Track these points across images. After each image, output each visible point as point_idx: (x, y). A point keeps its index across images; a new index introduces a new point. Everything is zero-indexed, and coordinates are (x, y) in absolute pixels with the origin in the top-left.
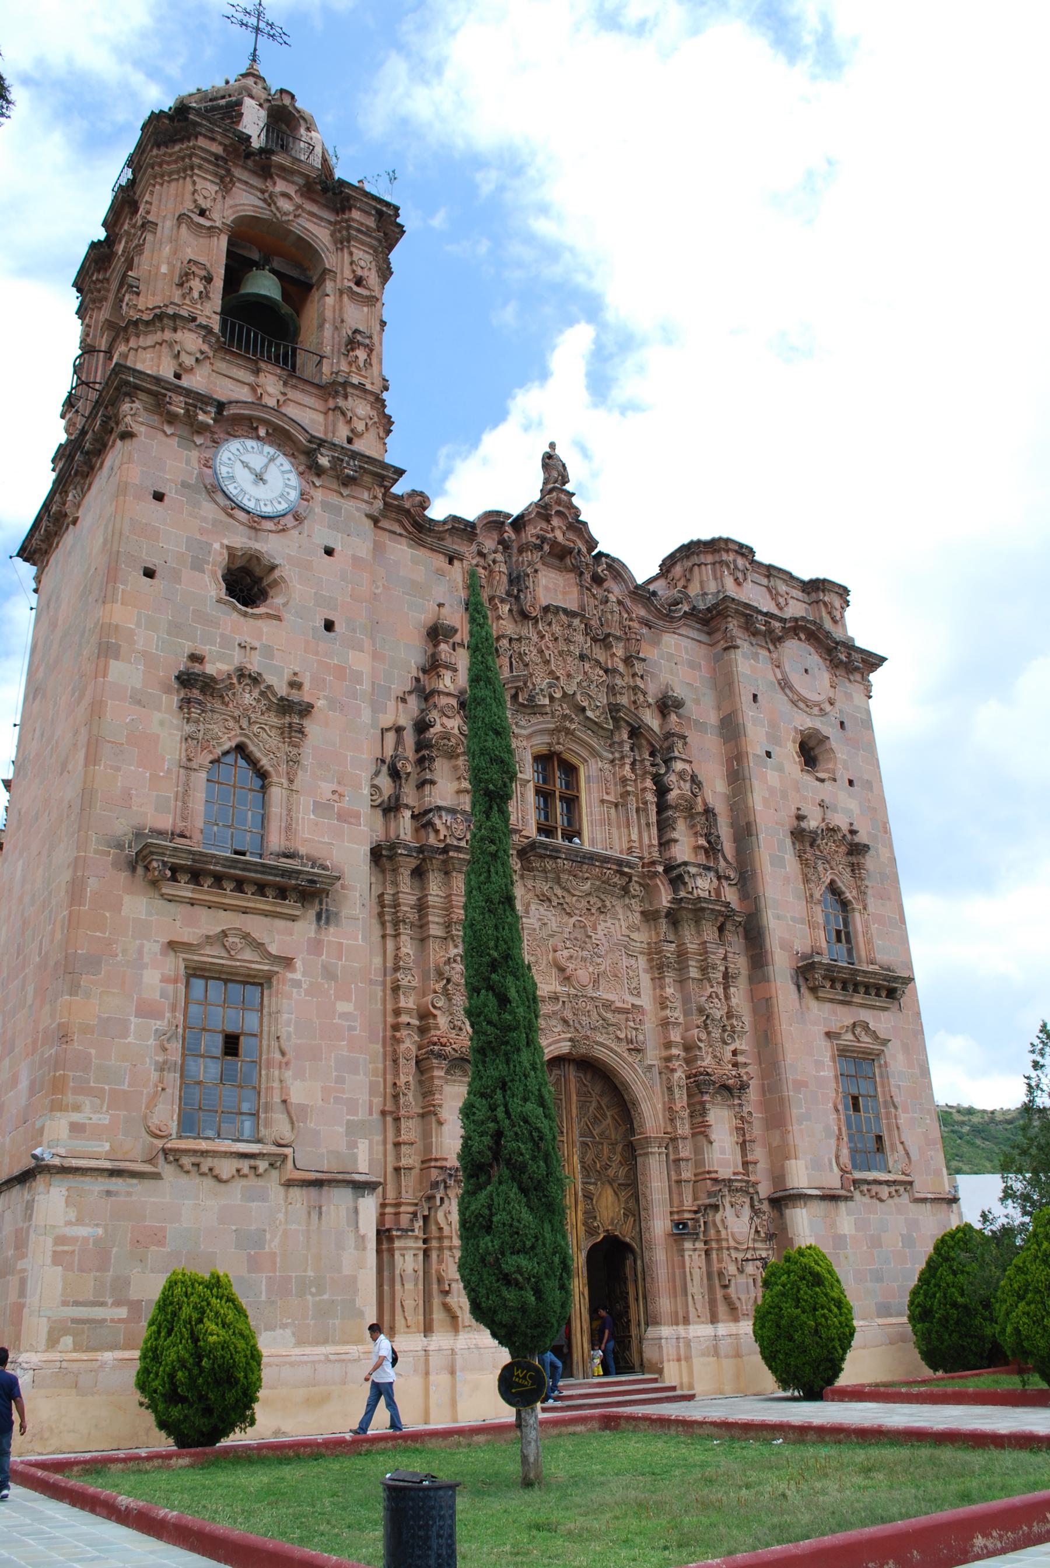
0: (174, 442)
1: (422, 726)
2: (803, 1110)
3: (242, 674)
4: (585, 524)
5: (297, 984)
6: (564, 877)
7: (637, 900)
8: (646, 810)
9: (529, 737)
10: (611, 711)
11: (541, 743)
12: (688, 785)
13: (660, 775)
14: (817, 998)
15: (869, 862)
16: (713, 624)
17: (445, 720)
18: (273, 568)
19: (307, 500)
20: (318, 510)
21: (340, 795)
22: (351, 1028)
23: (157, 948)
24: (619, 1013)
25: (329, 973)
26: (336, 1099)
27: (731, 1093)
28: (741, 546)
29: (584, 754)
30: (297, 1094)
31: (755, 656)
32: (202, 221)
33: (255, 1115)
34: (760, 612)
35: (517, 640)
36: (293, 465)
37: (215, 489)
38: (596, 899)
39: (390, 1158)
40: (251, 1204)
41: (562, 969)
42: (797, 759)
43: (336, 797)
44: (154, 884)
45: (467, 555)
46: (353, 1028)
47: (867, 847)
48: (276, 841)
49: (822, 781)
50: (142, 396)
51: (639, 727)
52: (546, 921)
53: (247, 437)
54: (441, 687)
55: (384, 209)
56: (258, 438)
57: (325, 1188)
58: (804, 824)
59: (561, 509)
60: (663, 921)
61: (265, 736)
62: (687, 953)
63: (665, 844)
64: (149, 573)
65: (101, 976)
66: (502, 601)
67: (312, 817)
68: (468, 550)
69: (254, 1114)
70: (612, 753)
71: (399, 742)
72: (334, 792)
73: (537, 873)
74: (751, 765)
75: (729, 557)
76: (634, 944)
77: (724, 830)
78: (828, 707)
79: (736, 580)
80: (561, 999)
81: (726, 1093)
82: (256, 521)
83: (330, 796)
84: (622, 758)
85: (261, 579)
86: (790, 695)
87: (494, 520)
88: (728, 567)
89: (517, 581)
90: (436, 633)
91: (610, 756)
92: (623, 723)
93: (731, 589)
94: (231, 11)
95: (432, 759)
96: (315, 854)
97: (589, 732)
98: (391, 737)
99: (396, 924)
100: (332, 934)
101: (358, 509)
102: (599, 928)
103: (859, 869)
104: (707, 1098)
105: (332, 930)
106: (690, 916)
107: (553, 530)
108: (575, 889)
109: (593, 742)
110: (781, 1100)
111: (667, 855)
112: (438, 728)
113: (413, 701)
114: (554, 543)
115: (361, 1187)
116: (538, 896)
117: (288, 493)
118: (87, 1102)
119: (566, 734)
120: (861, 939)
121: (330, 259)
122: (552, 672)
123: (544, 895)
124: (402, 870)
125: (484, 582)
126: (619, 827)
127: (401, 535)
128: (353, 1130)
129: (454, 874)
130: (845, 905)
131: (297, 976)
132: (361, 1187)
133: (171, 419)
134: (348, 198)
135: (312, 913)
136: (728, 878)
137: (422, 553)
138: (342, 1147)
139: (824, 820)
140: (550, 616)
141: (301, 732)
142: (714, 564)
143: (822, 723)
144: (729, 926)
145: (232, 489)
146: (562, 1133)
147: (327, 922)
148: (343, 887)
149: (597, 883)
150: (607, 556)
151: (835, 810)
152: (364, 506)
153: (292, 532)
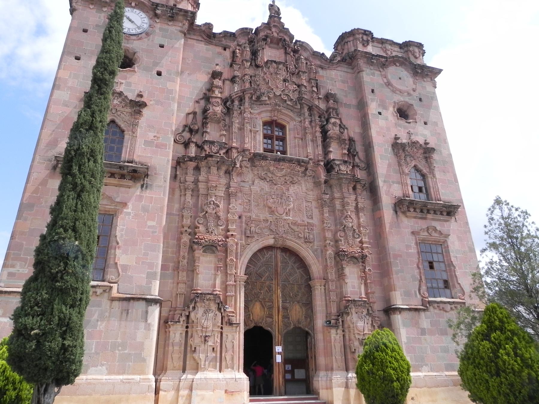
0: (94, 11)
1: (205, 111)
2: (399, 268)
4: (287, 29)
5: (129, 214)
6: (272, 168)
7: (311, 177)
8: (316, 140)
9: (259, 114)
10: (298, 100)
11: (266, 116)
12: (338, 128)
13: (324, 125)
14: (407, 217)
15: (435, 156)
16: (353, 64)
17: (214, 107)
18: (135, 53)
19: (152, 28)
20: (157, 31)
21: (158, 138)
22: (153, 232)
24: (301, 226)
25: (145, 209)
26: (143, 263)
27: (358, 260)
28: (365, 31)
29: (288, 119)
31: (373, 74)
35: (254, 76)
36: (147, 16)
38: (289, 178)
39: (175, 290)
40: (93, 308)
41: (270, 208)
42: (395, 115)
43: (156, 138)
45: (232, 46)
47: (433, 149)
49: (410, 123)
51: (312, 106)
52: (263, 188)
54: (214, 95)
56: (132, 7)
58: (399, 141)
59: (276, 24)
60: (323, 186)
61: (123, 116)
62: (335, 198)
63: (326, 153)
65: (33, 212)
66: (247, 61)
67: (143, 146)
68: (233, 45)
69: (102, 269)
70: (300, 118)
72: (154, 136)
73: (259, 168)
74: (370, 118)
75: (361, 36)
76: (310, 196)
77: (359, 148)
78: (412, 92)
79: (363, 45)
80: (269, 220)
81: (355, 260)
83: (153, 138)
84: (304, 119)
85: (132, 59)
86: (392, 88)
87: (245, 31)
88: (359, 40)
89: (254, 53)
91: (300, 119)
92: (305, 105)
93: (360, 48)
95: (207, 123)
96: (143, 160)
97: (290, 111)
98: (191, 116)
99: (185, 190)
100: (147, 194)
101: (176, 30)
102: (290, 190)
103: (430, 159)
104: (344, 262)
105: (148, 191)
106: (336, 182)
107: (272, 33)
108: (277, 173)
109: (291, 114)
110: (387, 263)
111: (327, 159)
112: (211, 110)
113: (203, 103)
115: (150, 302)
116: (259, 177)
117: (143, 25)
118: (18, 264)
119: (278, 112)
120: (432, 190)
122: (269, 87)
123: (262, 177)
124: (189, 167)
125: (238, 55)
126: (303, 148)
127: (201, 41)
128: (151, 276)
129: (212, 167)
130: (424, 176)
131: (129, 210)
132: (150, 302)
135: (139, 185)
136: (358, 166)
137: (210, 47)
138: (144, 284)
139: (410, 139)
140: (269, 65)
141: (139, 113)
142: (353, 40)
143: (409, 99)
144: (358, 186)
146: (272, 280)
148: (155, 174)
149: (289, 170)
150: (300, 41)
151: (417, 134)
152: (179, 28)
153: (145, 39)
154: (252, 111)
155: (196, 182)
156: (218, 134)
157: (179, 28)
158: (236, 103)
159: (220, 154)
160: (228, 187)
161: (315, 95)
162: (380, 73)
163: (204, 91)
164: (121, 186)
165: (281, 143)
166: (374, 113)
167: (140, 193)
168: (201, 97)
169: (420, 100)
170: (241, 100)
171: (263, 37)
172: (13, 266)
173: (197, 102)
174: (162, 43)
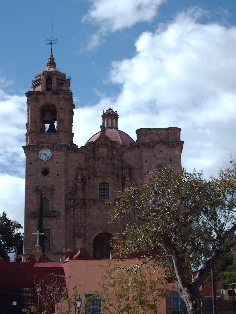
3: (44, 187)
5: (54, 229)
6: (101, 205)
11: (100, 181)
23: (35, 227)
30: (54, 243)
32: (34, 111)
33: (49, 246)
34: (147, 143)
37: (39, 159)
43: (59, 201)
44: (34, 219)
46: (62, 234)
48: (50, 210)
50: (27, 149)
53: (43, 148)
55: (65, 91)
57: (58, 255)
64: (31, 176)
66: (91, 159)
67: (56, 205)
71: (72, 189)
72: (59, 201)
74: (144, 175)
79: (144, 136)
82: (45, 162)
89: (94, 154)
90: (79, 168)
94: (46, 42)
98: (71, 188)
101: (62, 153)
105: (59, 221)
113: (75, 181)
114: (102, 145)
121: (56, 105)
127: (73, 153)
131: (54, 228)
133: (31, 151)
134: (58, 93)
135: (56, 219)
145: (41, 158)
147: (58, 220)
150: (114, 141)
152: (63, 152)
154: (94, 181)
155: (74, 214)
156: (81, 194)
157: (63, 152)
158: (87, 179)
159: (81, 203)
160: (85, 214)
161: (120, 168)
162: (151, 150)
163: (75, 176)
164: (51, 220)
165: (107, 190)
166: (146, 172)
167: (57, 221)
168: (74, 179)
169: (171, 160)
170: (89, 177)
171: (98, 145)
172: (26, 248)
173: (73, 182)
174: (57, 161)
